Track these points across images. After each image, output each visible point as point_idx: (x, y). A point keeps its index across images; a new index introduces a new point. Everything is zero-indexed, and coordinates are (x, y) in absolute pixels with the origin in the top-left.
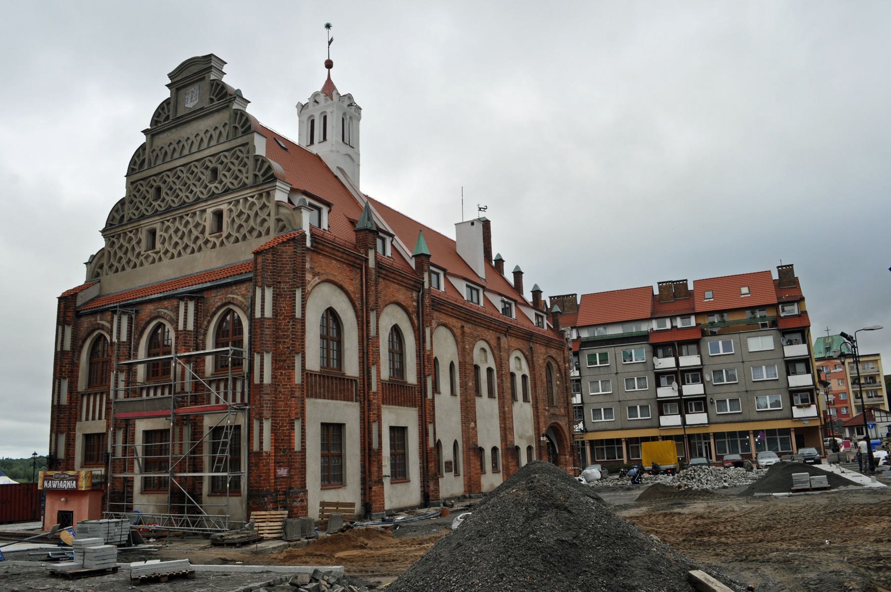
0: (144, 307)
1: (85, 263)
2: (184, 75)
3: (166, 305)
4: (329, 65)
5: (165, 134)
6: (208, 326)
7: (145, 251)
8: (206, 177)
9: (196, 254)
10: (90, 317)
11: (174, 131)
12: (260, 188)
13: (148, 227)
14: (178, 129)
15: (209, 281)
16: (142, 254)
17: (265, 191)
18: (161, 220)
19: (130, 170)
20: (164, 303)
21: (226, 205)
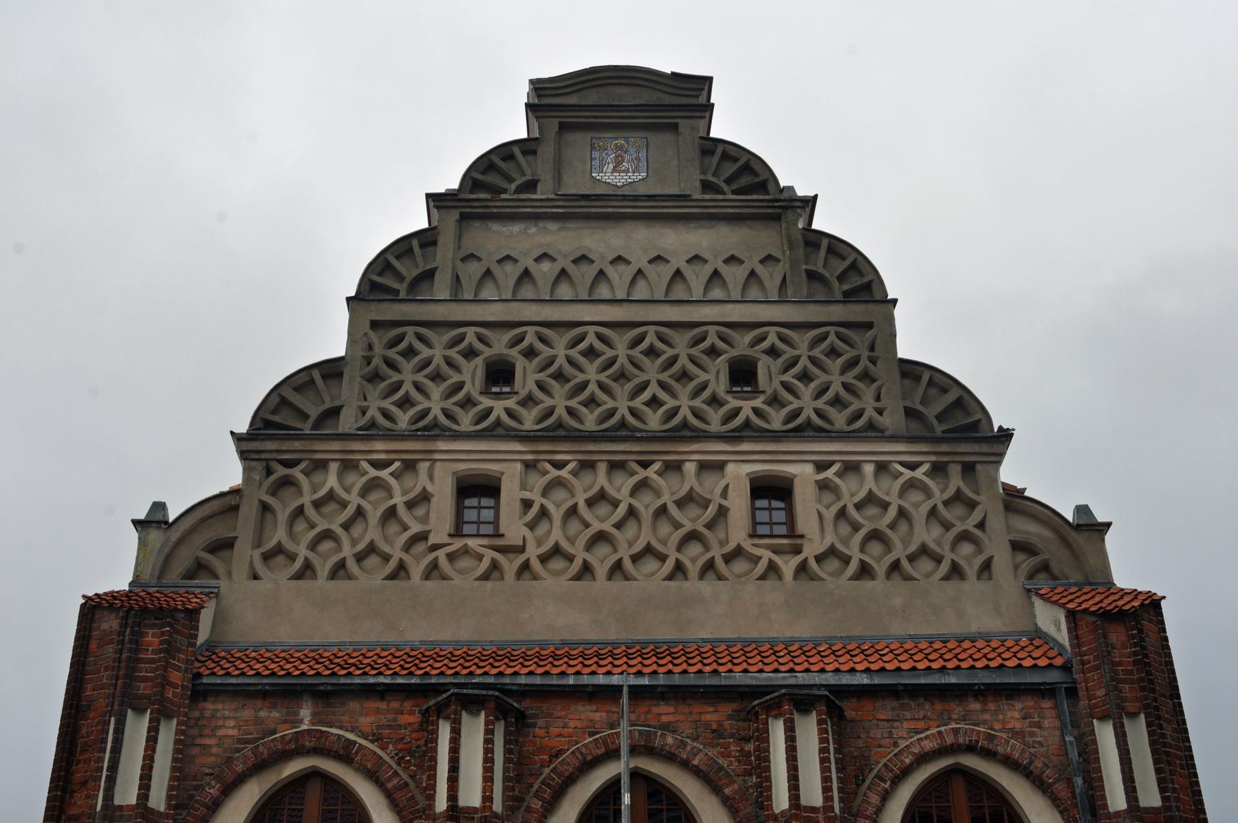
0: (557, 708)
1: (136, 523)
2: (592, 98)
3: (664, 719)
5: (516, 228)
6: (879, 810)
7: (450, 535)
8: (717, 377)
9: (692, 585)
10: (259, 703)
11: (552, 226)
12: (944, 448)
13: (462, 467)
14: (571, 225)
15: (867, 670)
16: (433, 540)
17: (958, 458)
18: (529, 457)
19: (367, 287)
20: (655, 710)
21: (809, 468)
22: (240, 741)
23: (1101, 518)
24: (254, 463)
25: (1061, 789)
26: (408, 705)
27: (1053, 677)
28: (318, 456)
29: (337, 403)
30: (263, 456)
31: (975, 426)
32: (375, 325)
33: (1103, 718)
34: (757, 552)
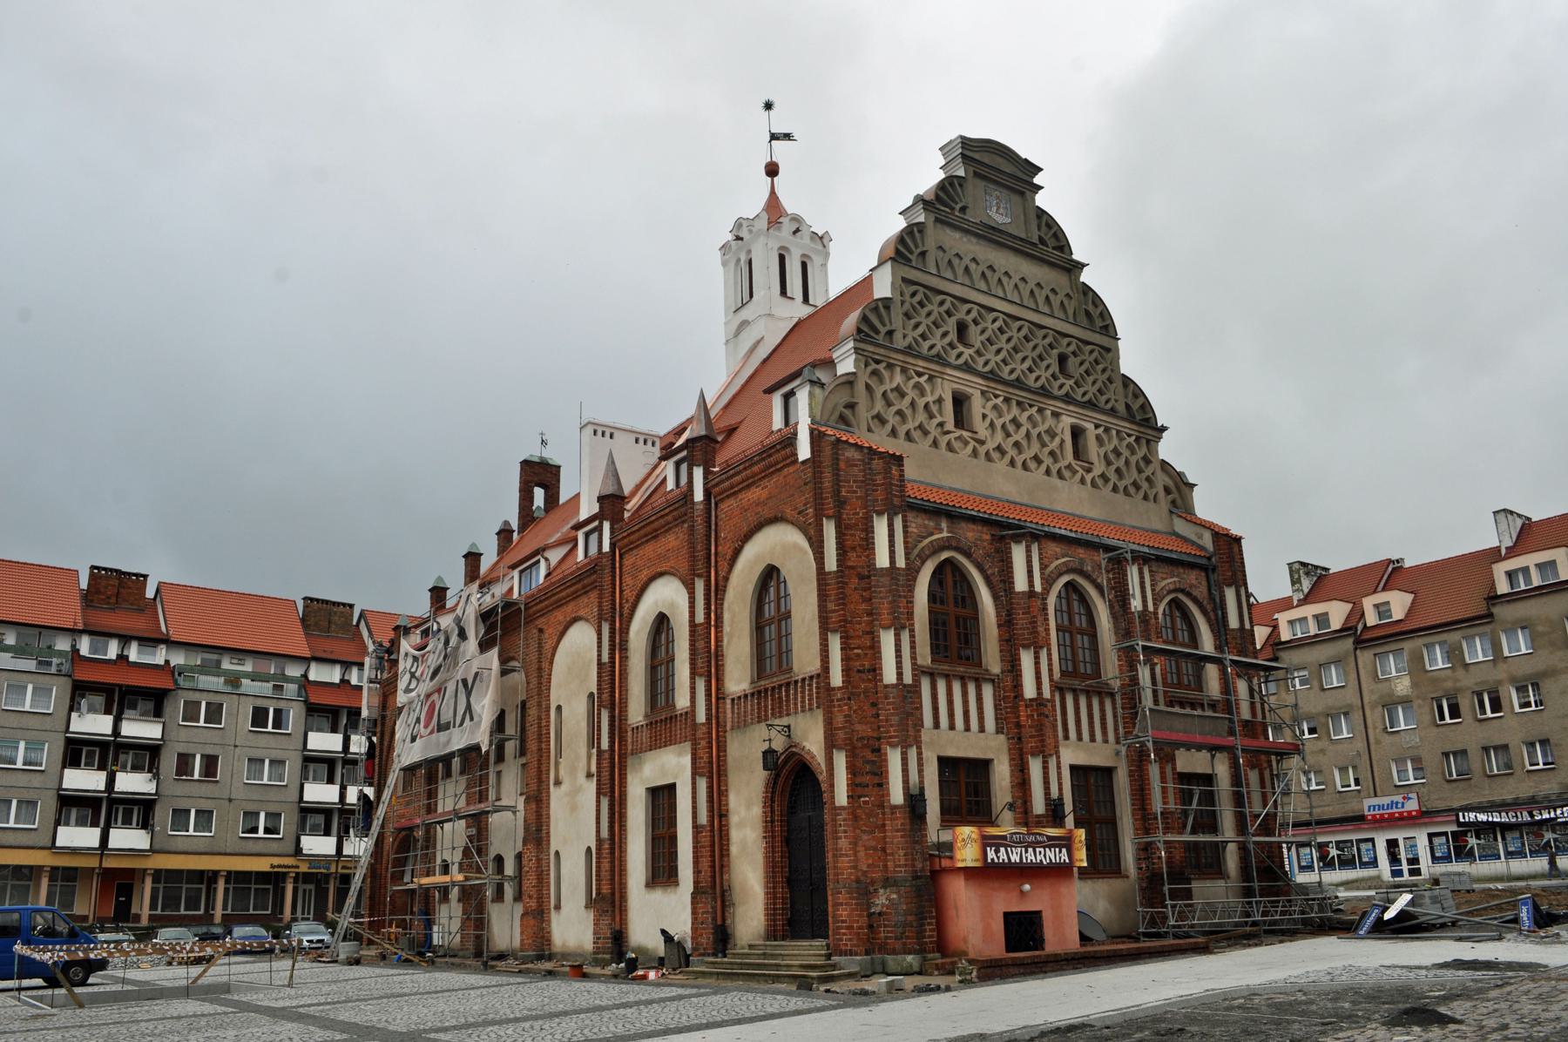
2: (986, 158)
4: (772, 170)
5: (957, 235)
10: (924, 516)
11: (974, 240)
13: (956, 386)
14: (982, 242)
18: (985, 389)
22: (919, 536)
23: (1191, 481)
24: (860, 357)
25: (1212, 615)
26: (985, 529)
27: (1204, 562)
28: (892, 361)
29: (893, 328)
30: (865, 353)
31: (1147, 420)
32: (904, 280)
33: (1229, 585)
34: (1078, 468)
